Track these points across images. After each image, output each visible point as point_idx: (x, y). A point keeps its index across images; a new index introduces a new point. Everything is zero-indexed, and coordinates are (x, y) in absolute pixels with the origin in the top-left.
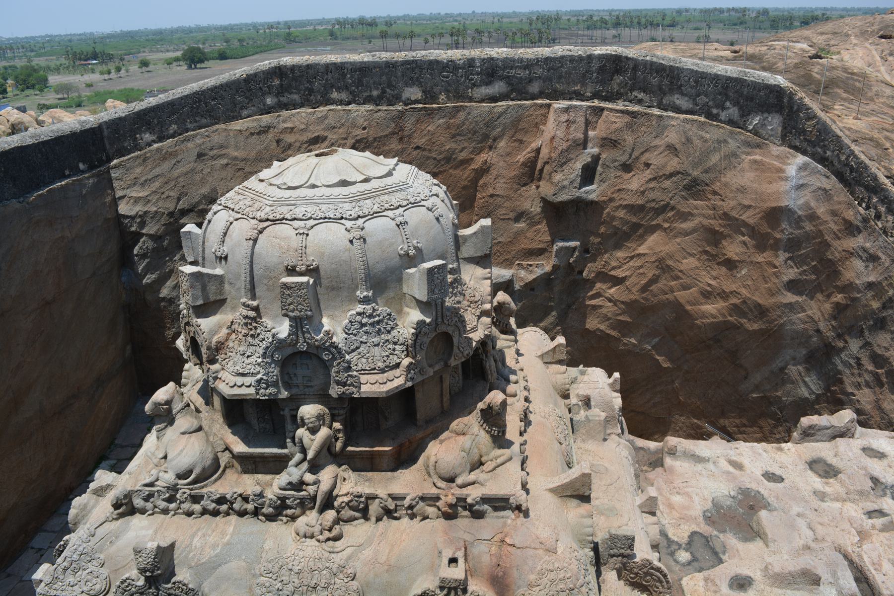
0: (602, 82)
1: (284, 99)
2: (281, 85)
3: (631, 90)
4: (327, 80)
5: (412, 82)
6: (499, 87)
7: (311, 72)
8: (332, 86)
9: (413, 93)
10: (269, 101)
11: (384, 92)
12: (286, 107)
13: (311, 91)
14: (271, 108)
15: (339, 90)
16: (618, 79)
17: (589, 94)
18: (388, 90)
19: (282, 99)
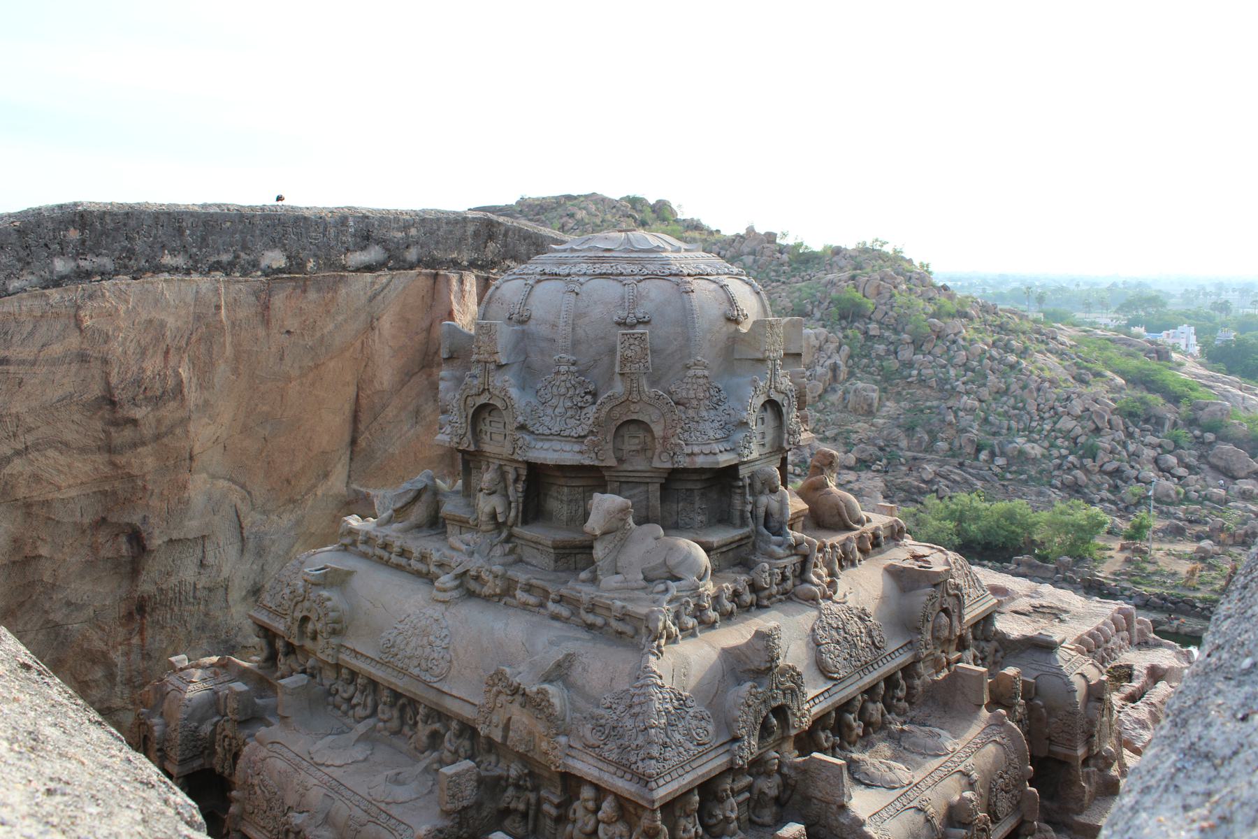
0: (477, 249)
1: (85, 264)
2: (83, 242)
3: (504, 259)
4: (155, 237)
5: (274, 244)
6: (374, 254)
7: (132, 223)
8: (163, 247)
9: (275, 259)
10: (61, 265)
11: (237, 257)
12: (87, 275)
13: (131, 253)
14: (63, 278)
15: (173, 252)
16: (491, 245)
17: (465, 263)
18: (242, 254)
19: (82, 263)
